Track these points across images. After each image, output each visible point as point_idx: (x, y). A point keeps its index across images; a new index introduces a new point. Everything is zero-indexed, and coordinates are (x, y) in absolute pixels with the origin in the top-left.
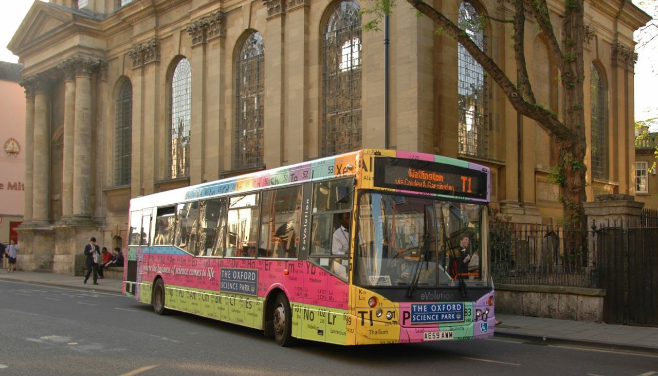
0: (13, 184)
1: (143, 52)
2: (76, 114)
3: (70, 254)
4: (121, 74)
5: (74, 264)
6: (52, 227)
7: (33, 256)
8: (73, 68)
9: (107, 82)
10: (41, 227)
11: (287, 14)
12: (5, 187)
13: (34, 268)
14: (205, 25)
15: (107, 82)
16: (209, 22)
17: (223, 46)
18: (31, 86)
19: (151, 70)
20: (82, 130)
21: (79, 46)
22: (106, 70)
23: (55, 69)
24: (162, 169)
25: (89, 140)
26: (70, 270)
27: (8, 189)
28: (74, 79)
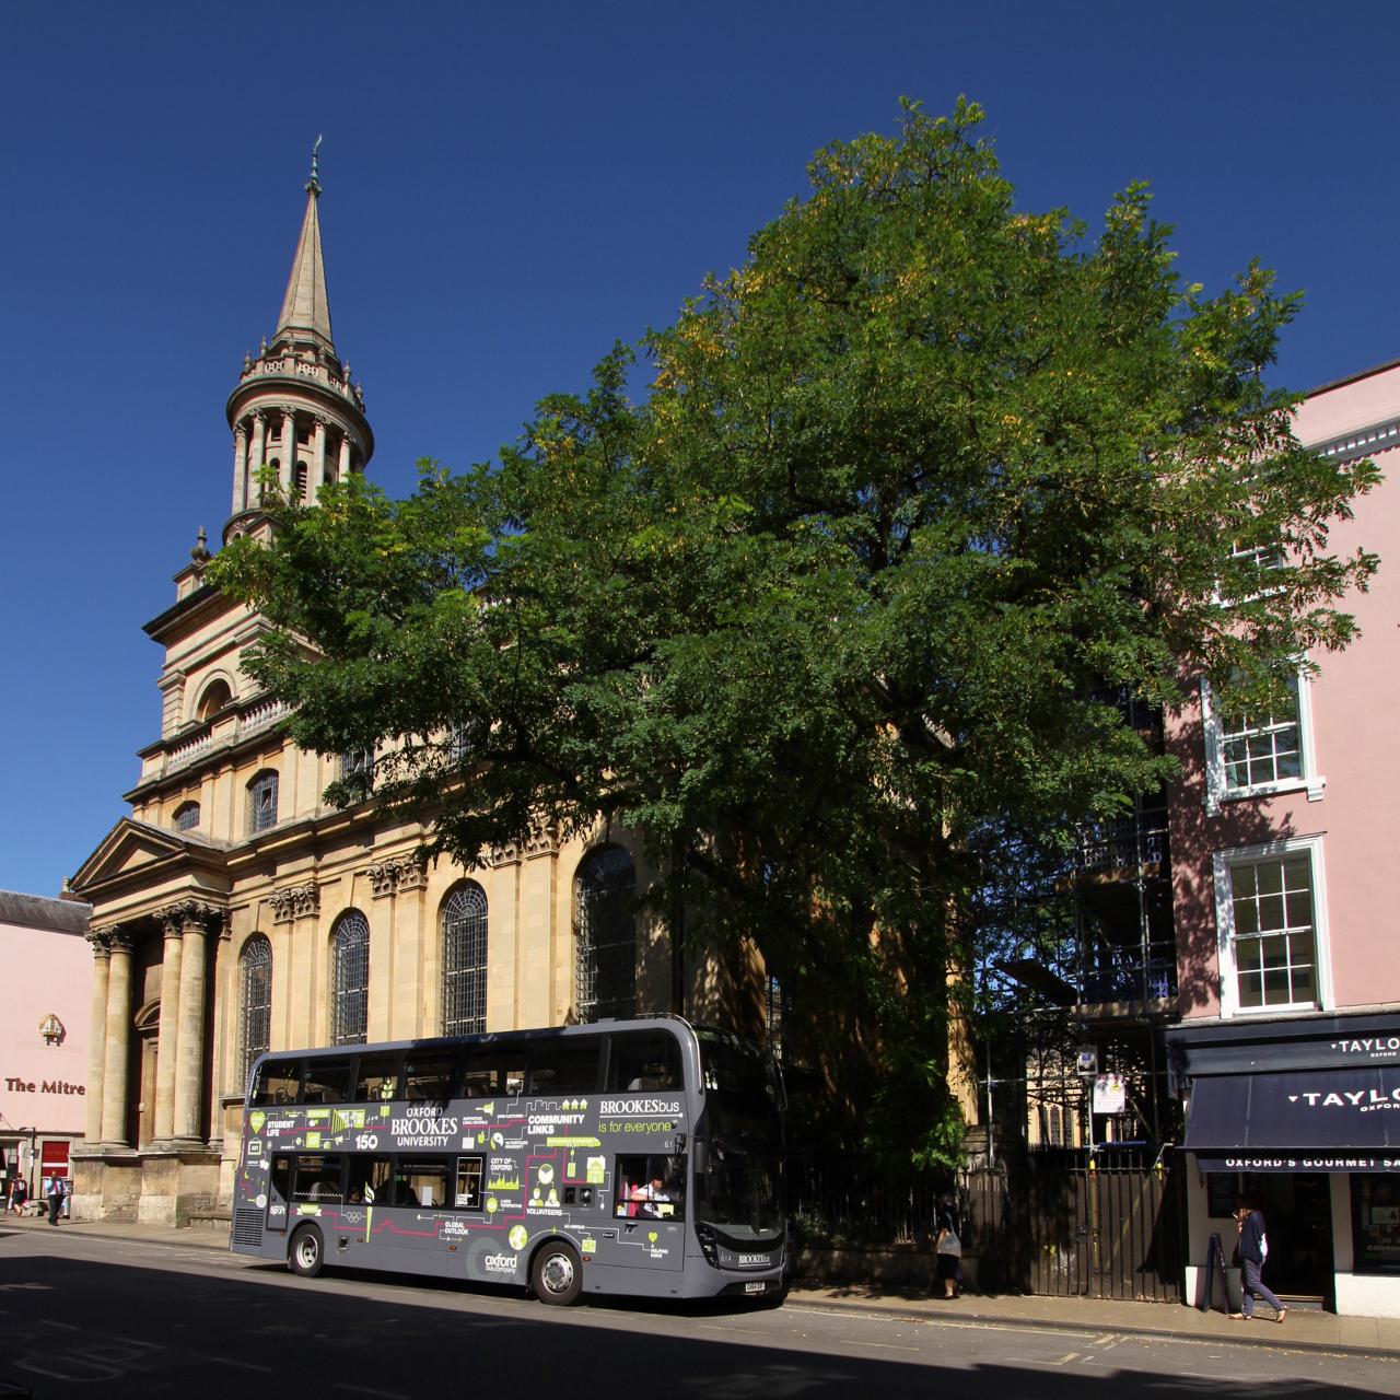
0: (50, 1085)
1: (291, 901)
2: (183, 986)
3: (167, 1194)
4: (254, 930)
5: (175, 1209)
6: (136, 1154)
7: (101, 1197)
8: (177, 920)
9: (229, 939)
11: (525, 862)
12: (39, 1088)
13: (102, 1215)
15: (229, 939)
18: (104, 941)
20: (192, 1010)
21: (191, 888)
22: (229, 925)
23: (149, 917)
26: (169, 1219)
28: (180, 935)
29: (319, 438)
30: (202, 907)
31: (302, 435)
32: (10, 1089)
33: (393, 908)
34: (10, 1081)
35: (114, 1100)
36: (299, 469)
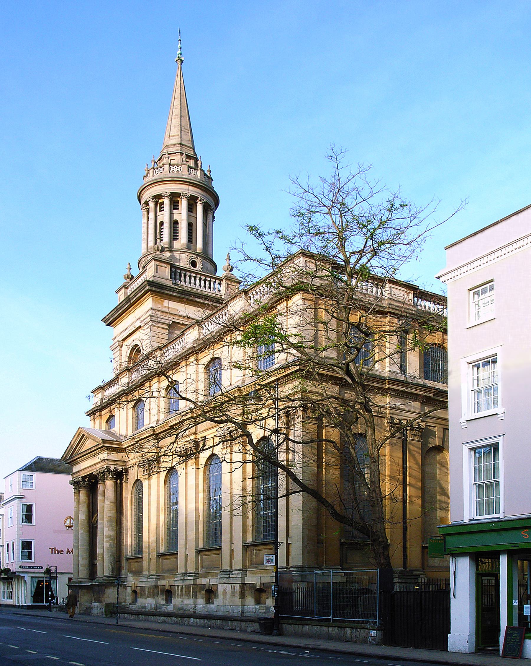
0: (70, 550)
3: (101, 602)
10: (83, 583)
12: (65, 552)
14: (185, 449)
16: (188, 447)
17: (197, 464)
19: (154, 477)
24: (162, 545)
25: (114, 524)
27: (67, 554)
29: (184, 204)
30: (112, 468)
31: (175, 205)
32: (52, 553)
33: (186, 468)
34: (52, 549)
35: (83, 559)
36: (174, 224)
